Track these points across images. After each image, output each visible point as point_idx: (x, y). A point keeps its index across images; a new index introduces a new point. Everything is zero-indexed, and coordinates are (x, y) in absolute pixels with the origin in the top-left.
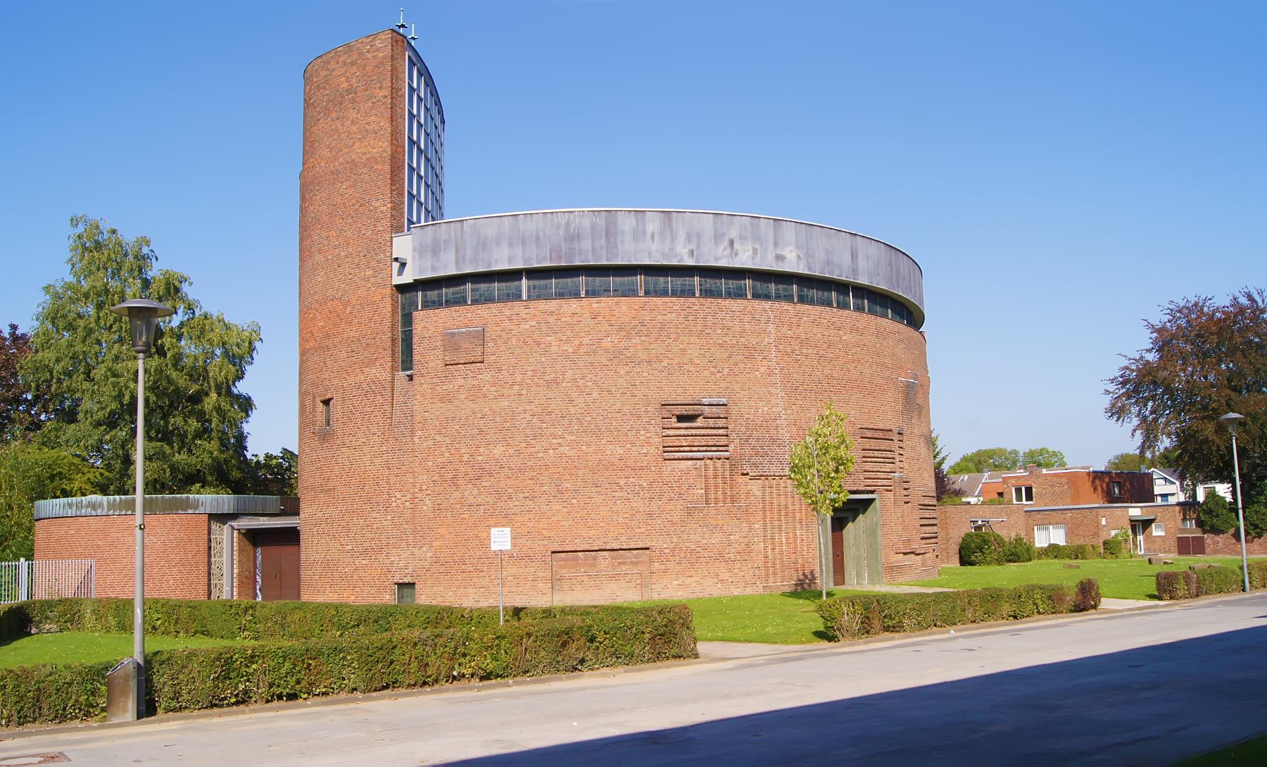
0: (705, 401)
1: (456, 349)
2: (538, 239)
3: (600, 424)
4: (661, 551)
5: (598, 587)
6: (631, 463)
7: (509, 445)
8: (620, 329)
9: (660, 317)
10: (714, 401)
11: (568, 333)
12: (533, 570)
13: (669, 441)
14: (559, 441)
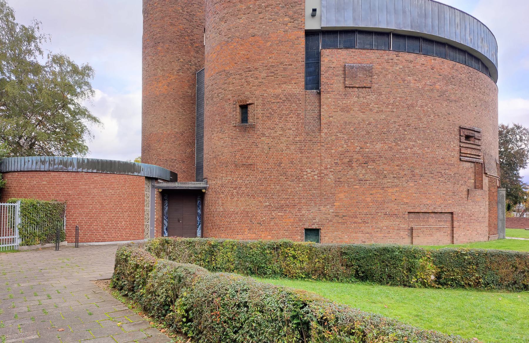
1: (354, 77)
2: (404, 12)
5: (431, 235)
7: (385, 143)
8: (444, 78)
11: (420, 76)
14: (414, 143)
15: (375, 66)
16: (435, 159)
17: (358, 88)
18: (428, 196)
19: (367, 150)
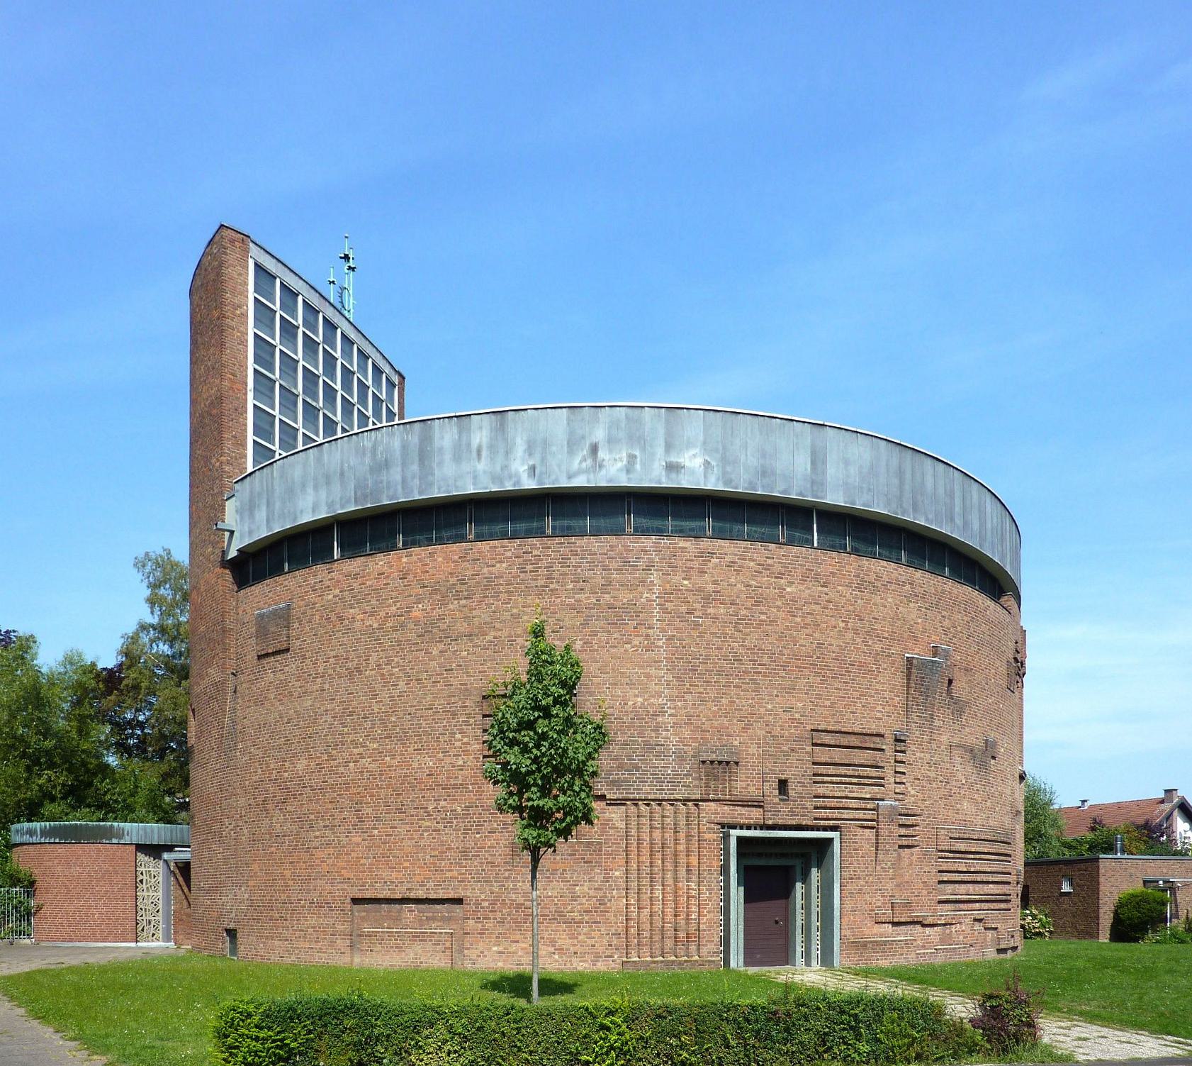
5: (400, 949)
6: (442, 778)
8: (435, 591)
9: (485, 570)
11: (374, 602)
12: (332, 921)
15: (298, 603)
16: (411, 779)
17: (274, 654)
19: (286, 775)
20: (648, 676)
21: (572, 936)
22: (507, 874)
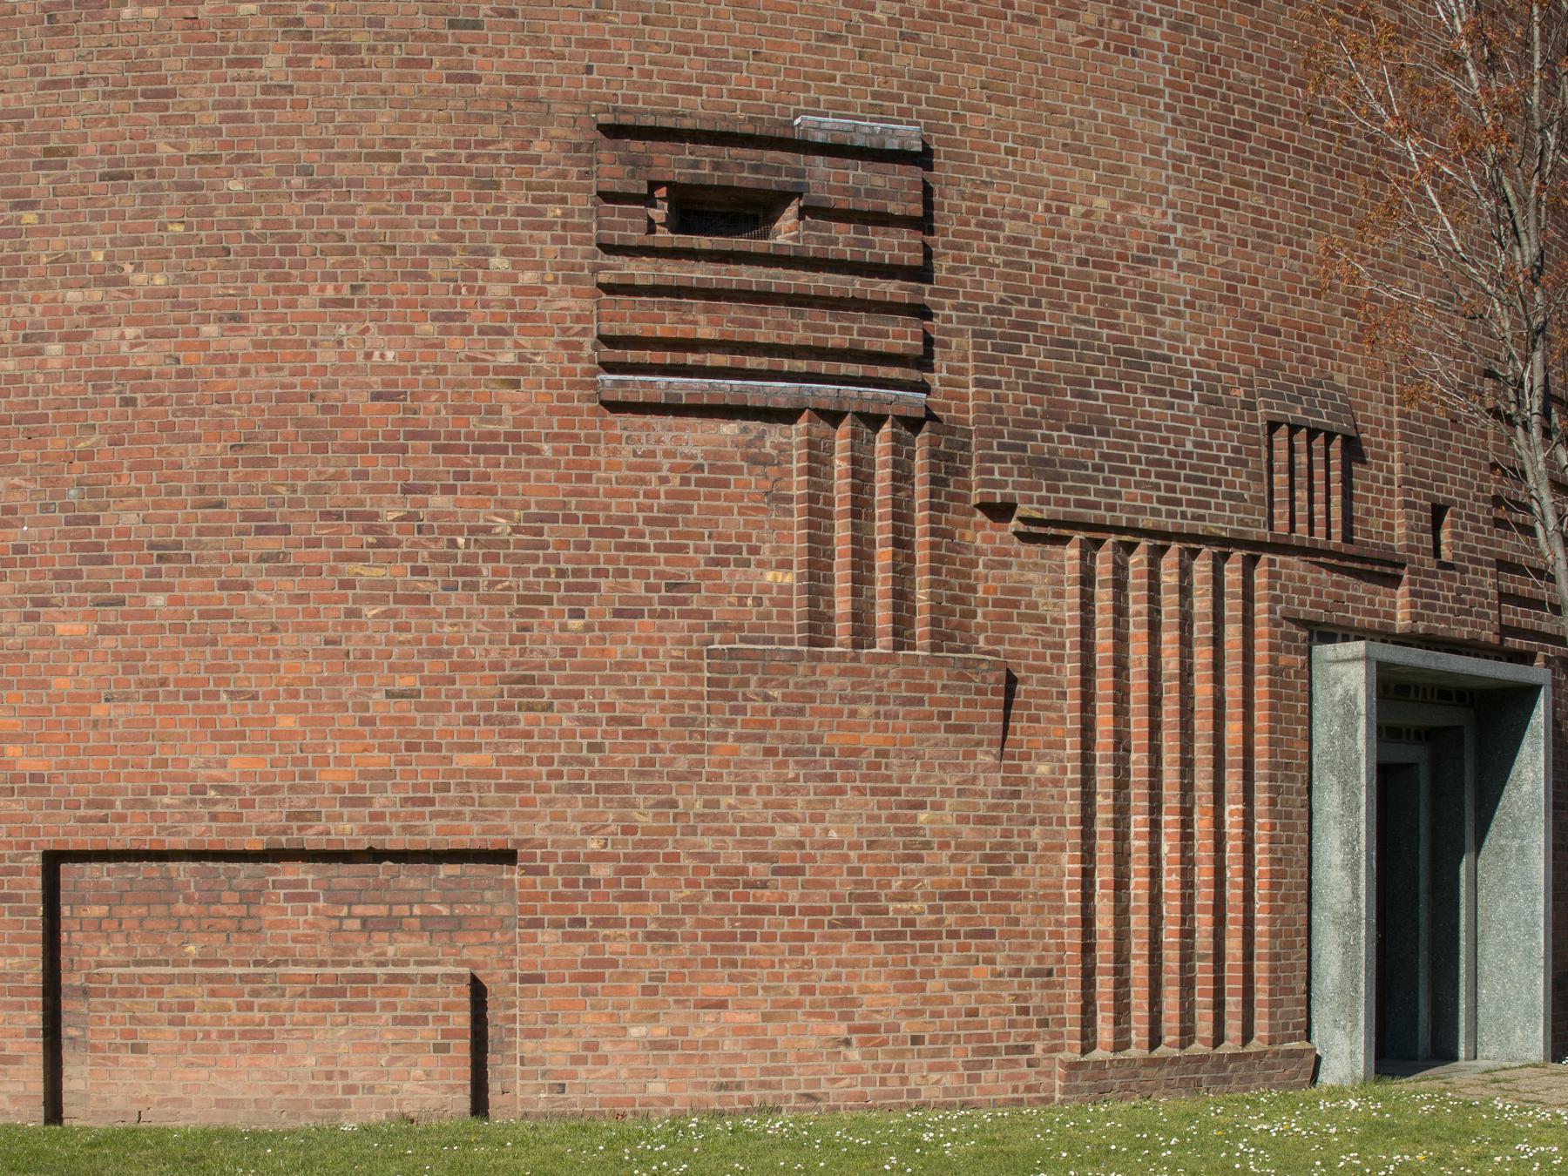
0: (823, 127)
3: (293, 211)
4: (575, 866)
5: (262, 1040)
6: (435, 412)
10: (867, 131)
13: (632, 318)
14: (96, 295)
16: (307, 410)
18: (227, 719)
20: (1124, 132)
21: (909, 982)
22: (682, 763)
